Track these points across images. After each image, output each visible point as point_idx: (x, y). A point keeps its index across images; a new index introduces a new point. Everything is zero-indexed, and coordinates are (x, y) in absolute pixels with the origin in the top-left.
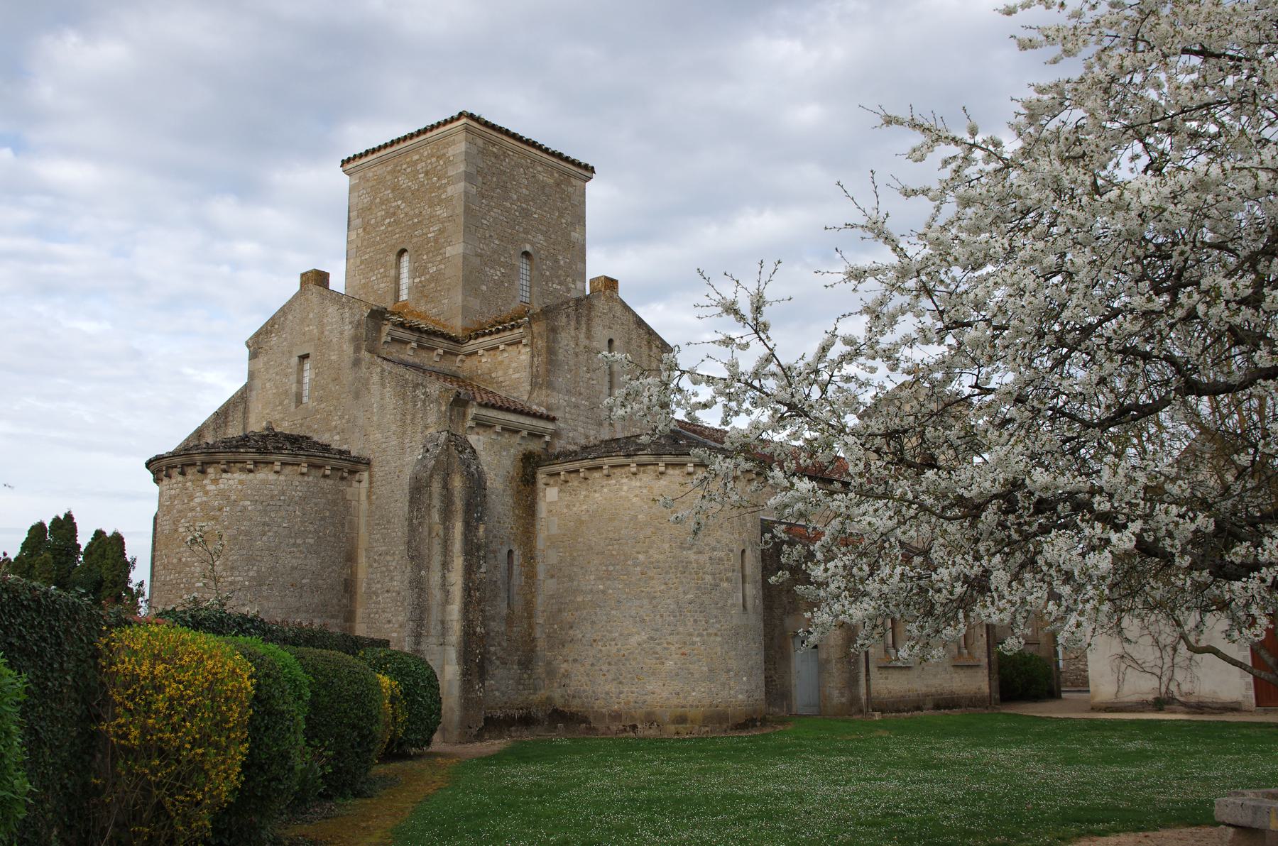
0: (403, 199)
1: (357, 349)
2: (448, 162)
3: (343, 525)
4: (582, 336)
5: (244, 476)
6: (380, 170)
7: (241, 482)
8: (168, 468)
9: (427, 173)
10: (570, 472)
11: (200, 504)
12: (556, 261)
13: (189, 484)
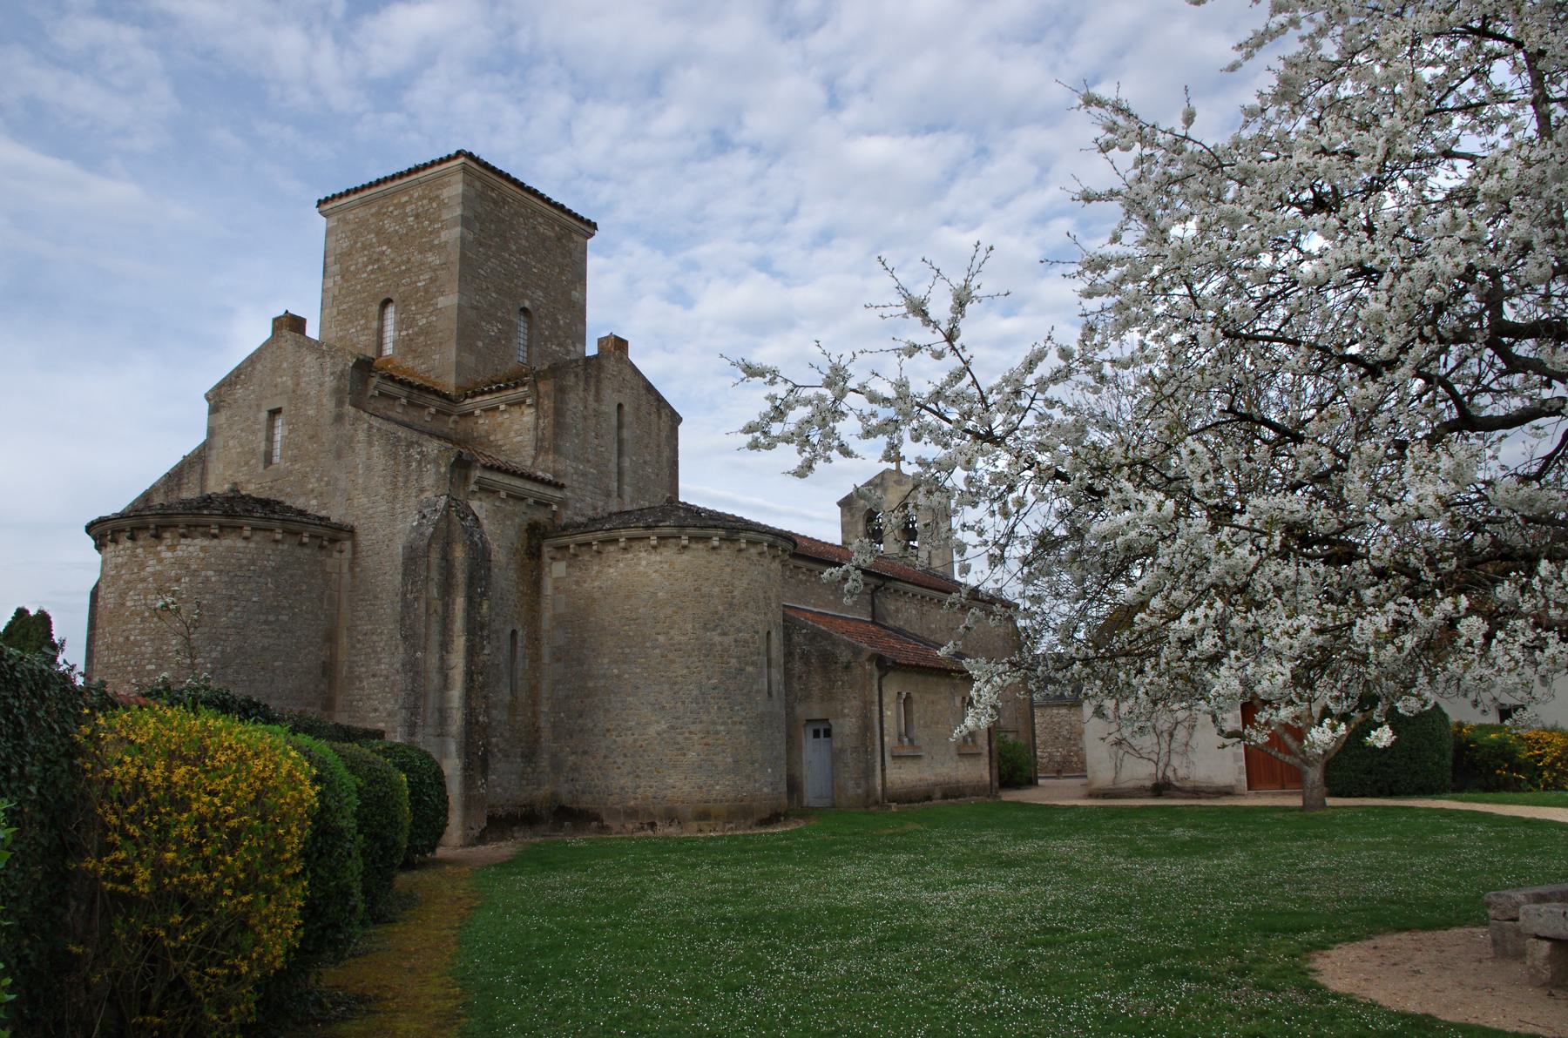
0: (388, 243)
1: (340, 403)
2: (442, 205)
3: (321, 600)
4: (591, 398)
5: (206, 543)
6: (362, 212)
7: (203, 549)
8: (113, 533)
9: (417, 216)
10: (580, 545)
11: (153, 574)
12: (556, 321)
13: (139, 550)
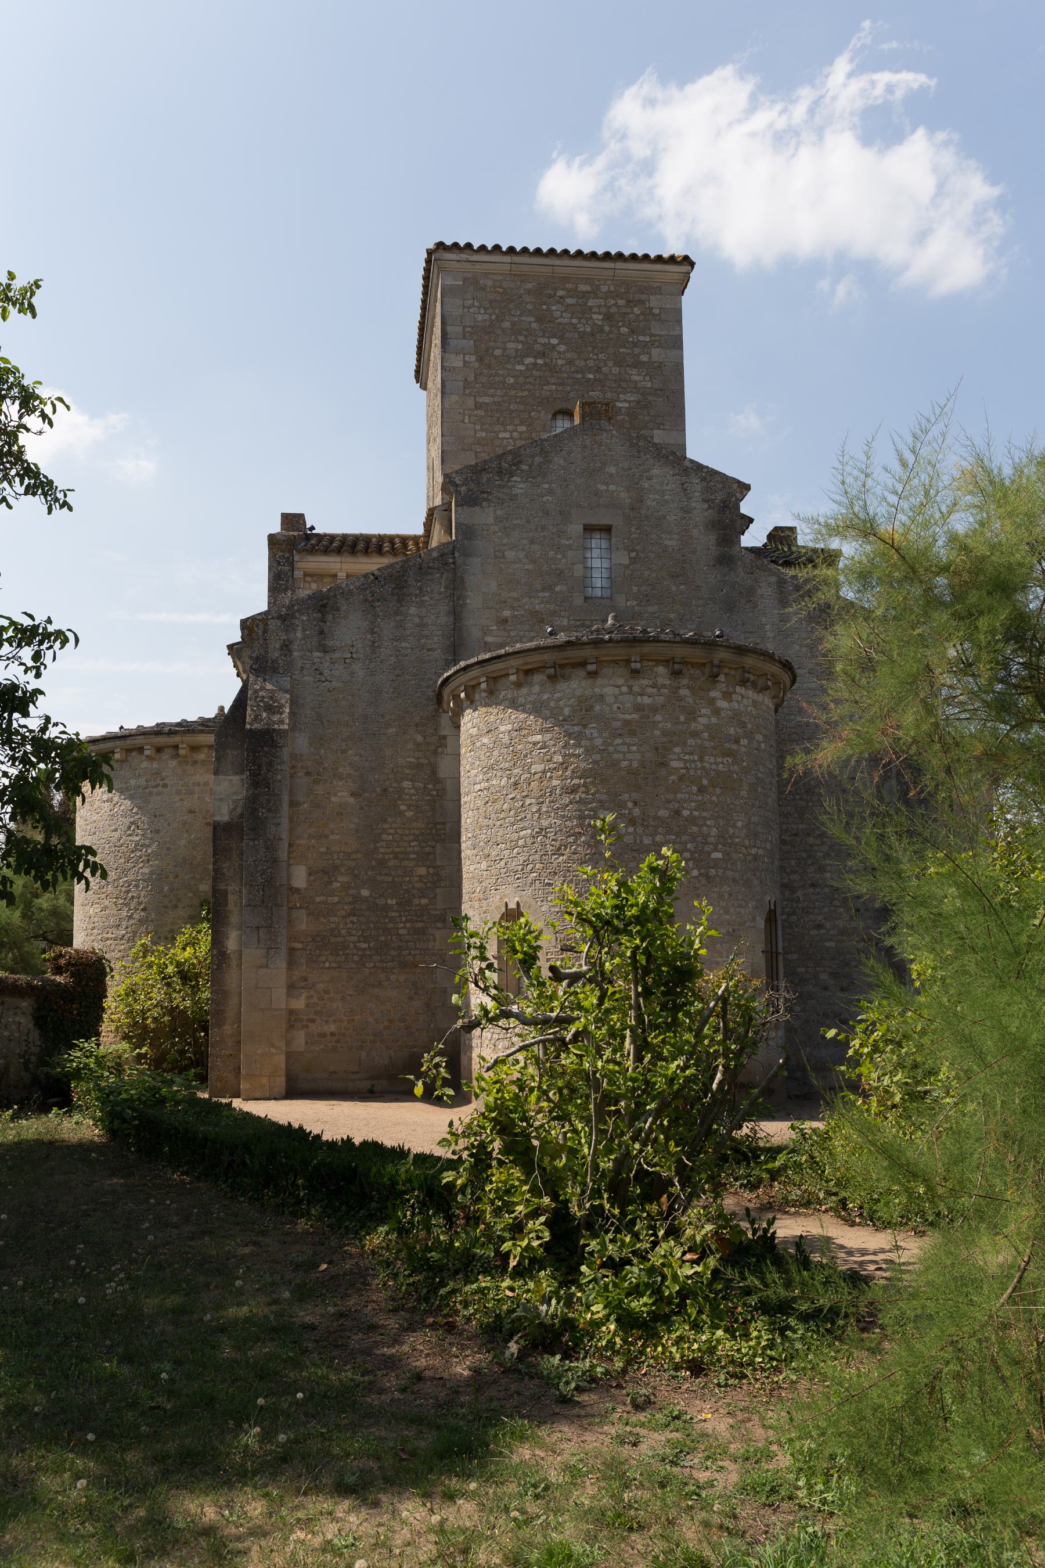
9: (608, 317)
11: (708, 728)
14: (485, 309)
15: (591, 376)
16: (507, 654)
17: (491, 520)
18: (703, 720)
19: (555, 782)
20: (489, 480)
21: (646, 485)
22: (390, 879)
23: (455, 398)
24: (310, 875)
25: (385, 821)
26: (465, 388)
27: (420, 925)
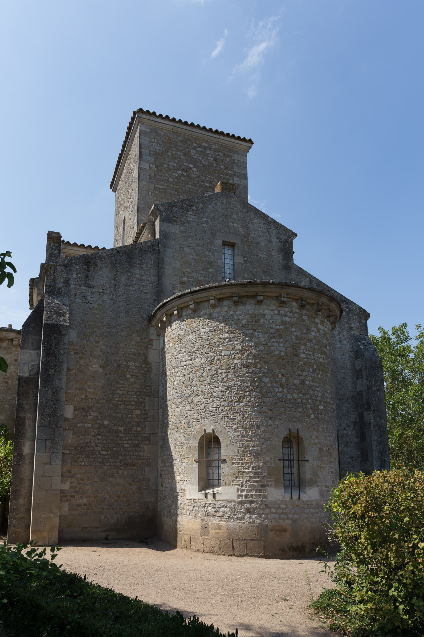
9: (215, 160)
11: (315, 337)
14: (160, 145)
15: (208, 185)
16: (211, 288)
17: (177, 231)
18: (313, 334)
19: (237, 361)
20: (177, 211)
21: (251, 227)
22: (120, 415)
23: (144, 183)
24: (75, 410)
25: (119, 383)
26: (149, 179)
27: (136, 442)
